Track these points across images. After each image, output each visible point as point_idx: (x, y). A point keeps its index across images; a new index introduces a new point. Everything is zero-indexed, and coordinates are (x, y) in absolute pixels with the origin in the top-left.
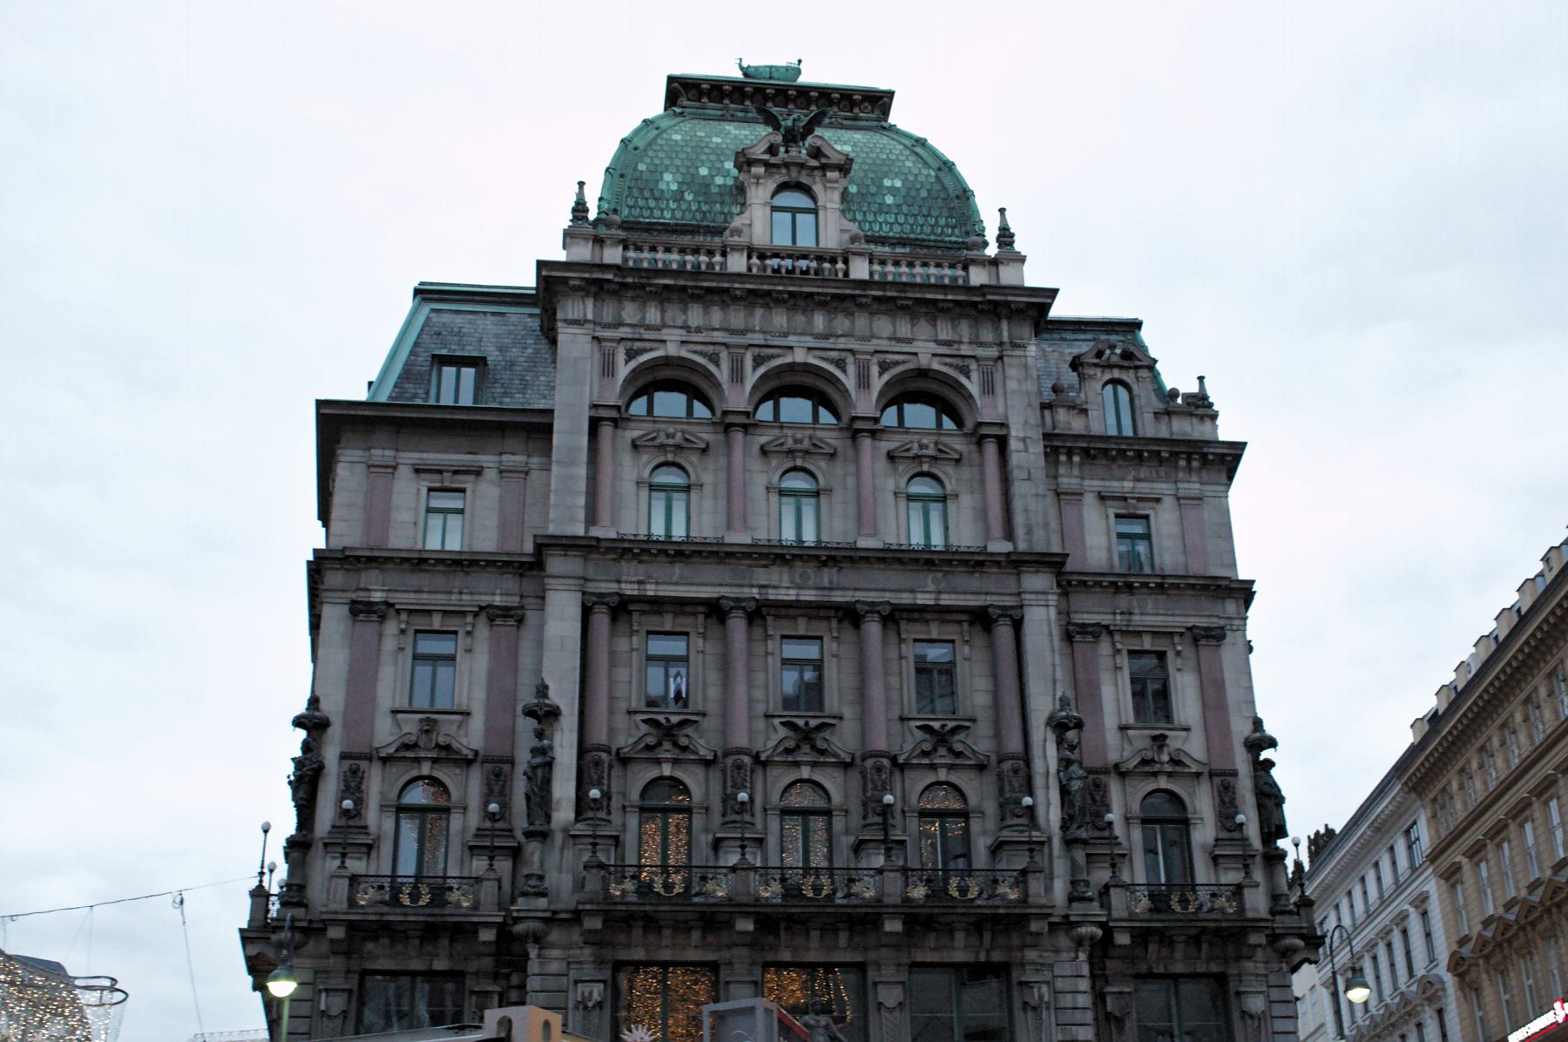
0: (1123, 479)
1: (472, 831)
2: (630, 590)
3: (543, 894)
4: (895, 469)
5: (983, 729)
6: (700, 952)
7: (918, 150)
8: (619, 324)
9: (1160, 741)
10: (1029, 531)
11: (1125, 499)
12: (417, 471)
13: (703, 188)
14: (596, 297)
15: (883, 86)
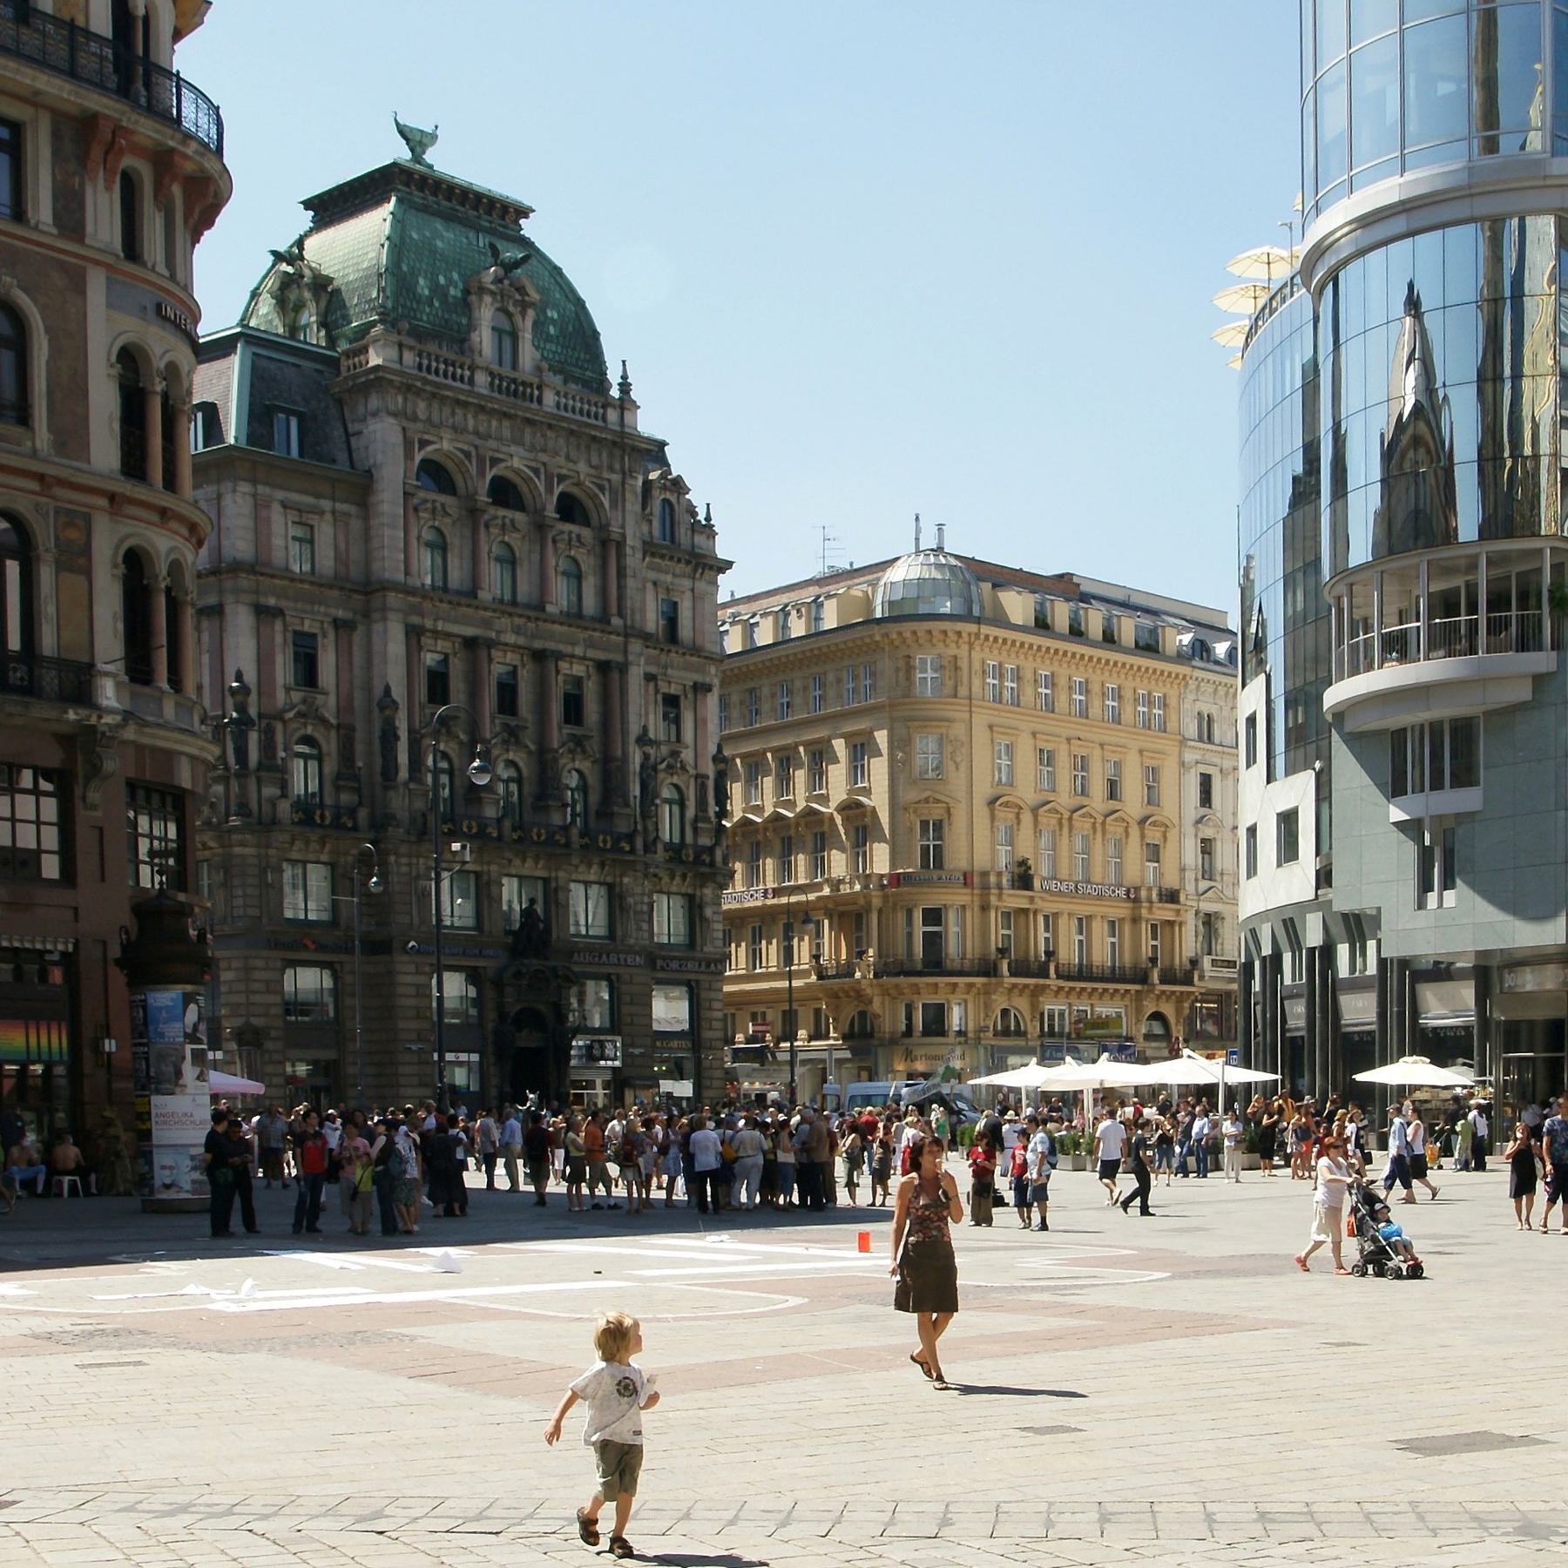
2: (429, 624)
3: (397, 826)
8: (415, 419)
9: (675, 754)
12: (284, 506)
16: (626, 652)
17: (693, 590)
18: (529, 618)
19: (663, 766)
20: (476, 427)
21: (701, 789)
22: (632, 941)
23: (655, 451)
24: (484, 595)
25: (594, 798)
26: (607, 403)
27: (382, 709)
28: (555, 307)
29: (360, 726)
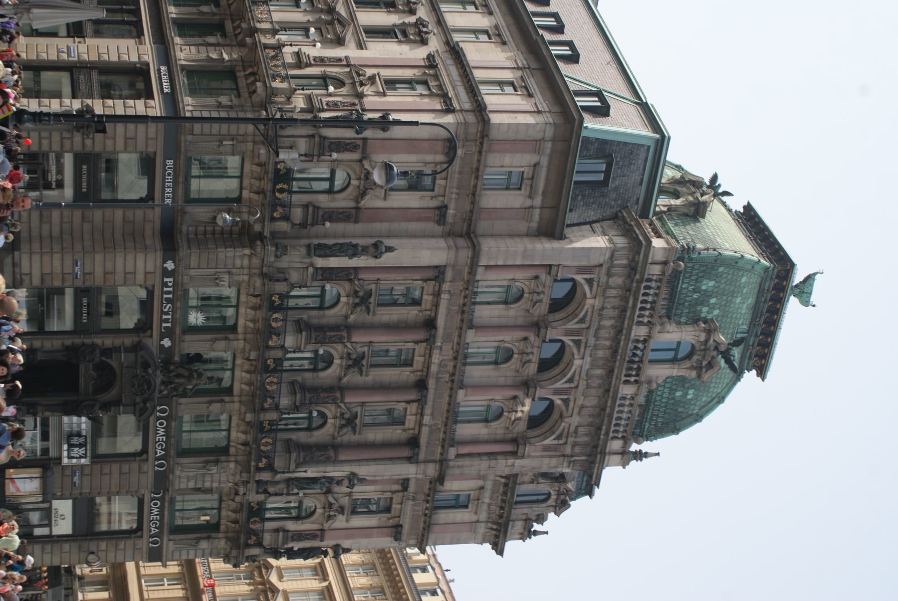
0: (491, 498)
1: (317, 205)
2: (446, 286)
3: (276, 256)
4: (506, 400)
5: (355, 438)
7: (715, 401)
8: (609, 275)
9: (341, 510)
10: (459, 467)
11: (478, 499)
12: (536, 165)
13: (703, 302)
14: (629, 265)
15: (770, 374)
16: (426, 461)
17: (478, 521)
18: (453, 374)
19: (332, 500)
20: (604, 327)
21: (311, 536)
22: (178, 473)
23: (588, 488)
24: (470, 336)
25: (302, 437)
26: (626, 442)
27: (376, 245)
28: (696, 397)
29: (359, 227)
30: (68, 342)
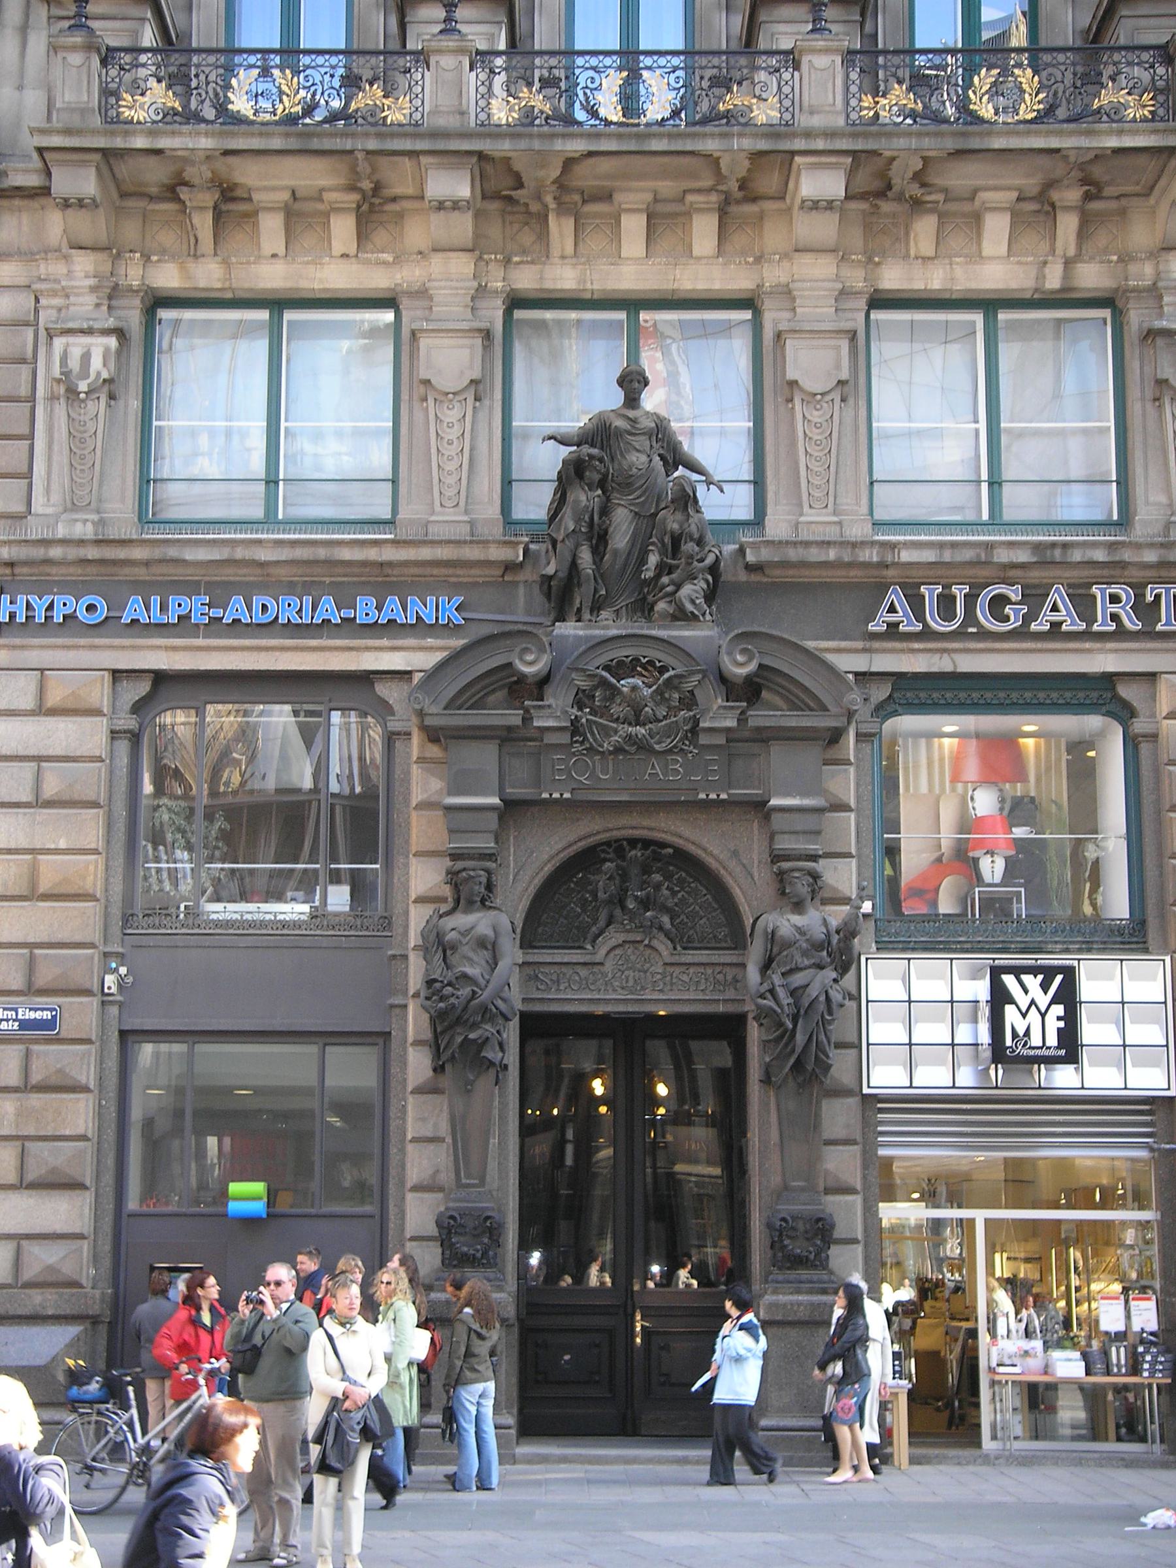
6: (353, 267)
30: (417, 1064)
